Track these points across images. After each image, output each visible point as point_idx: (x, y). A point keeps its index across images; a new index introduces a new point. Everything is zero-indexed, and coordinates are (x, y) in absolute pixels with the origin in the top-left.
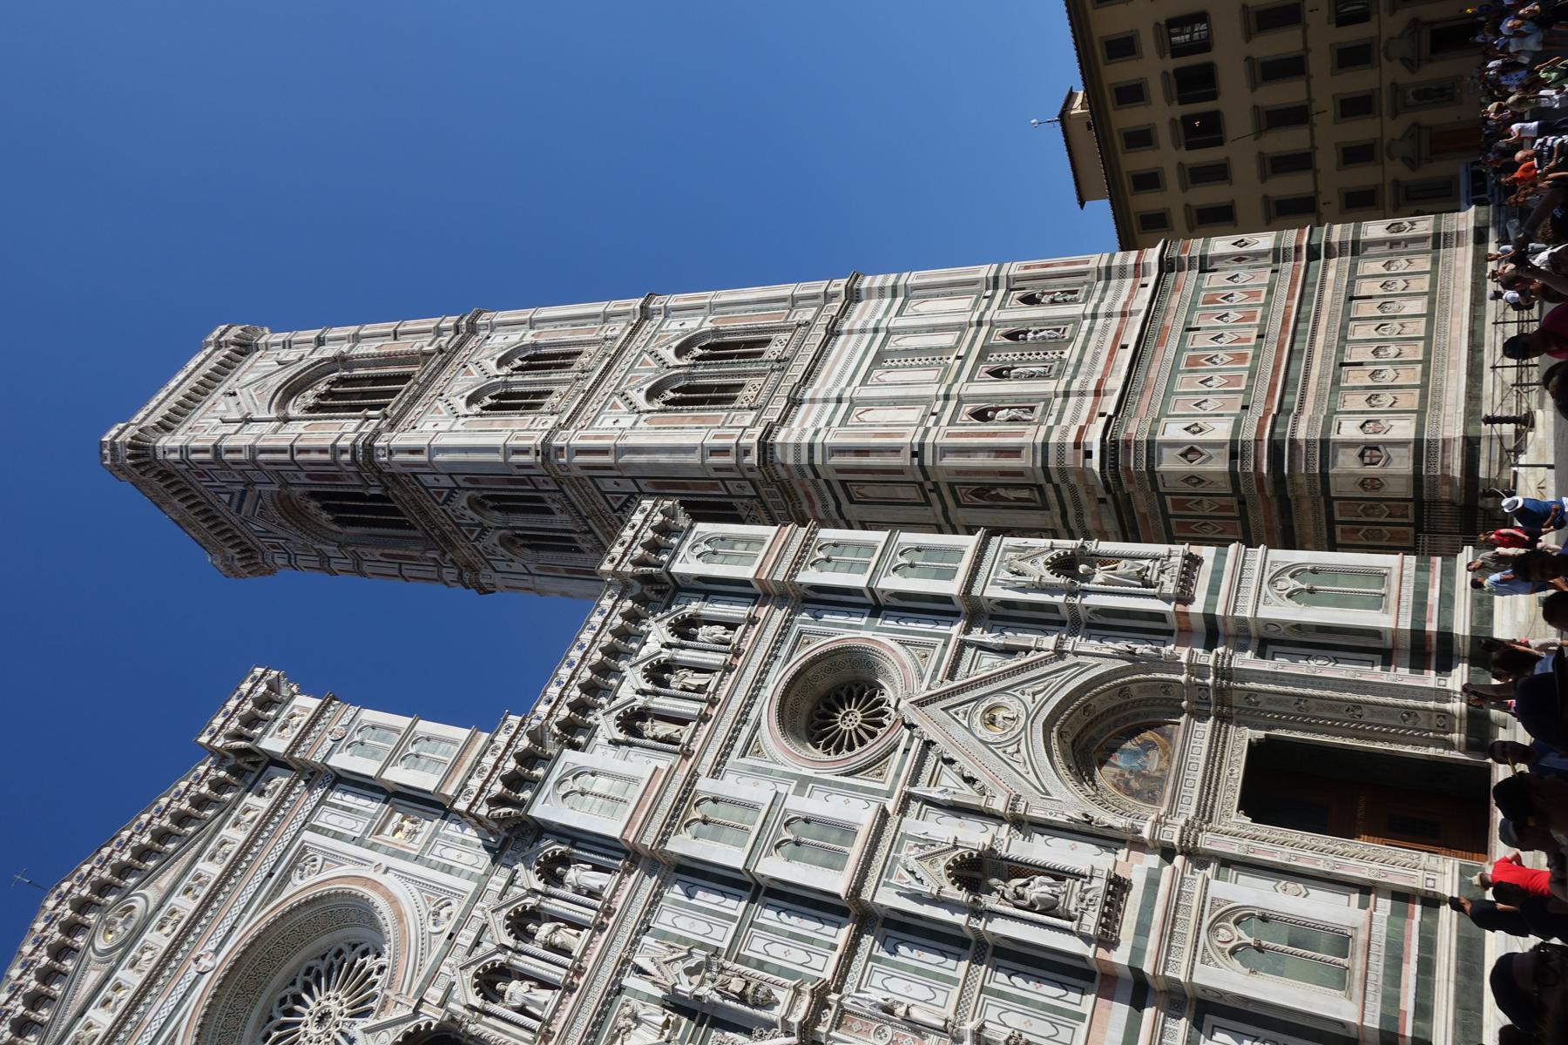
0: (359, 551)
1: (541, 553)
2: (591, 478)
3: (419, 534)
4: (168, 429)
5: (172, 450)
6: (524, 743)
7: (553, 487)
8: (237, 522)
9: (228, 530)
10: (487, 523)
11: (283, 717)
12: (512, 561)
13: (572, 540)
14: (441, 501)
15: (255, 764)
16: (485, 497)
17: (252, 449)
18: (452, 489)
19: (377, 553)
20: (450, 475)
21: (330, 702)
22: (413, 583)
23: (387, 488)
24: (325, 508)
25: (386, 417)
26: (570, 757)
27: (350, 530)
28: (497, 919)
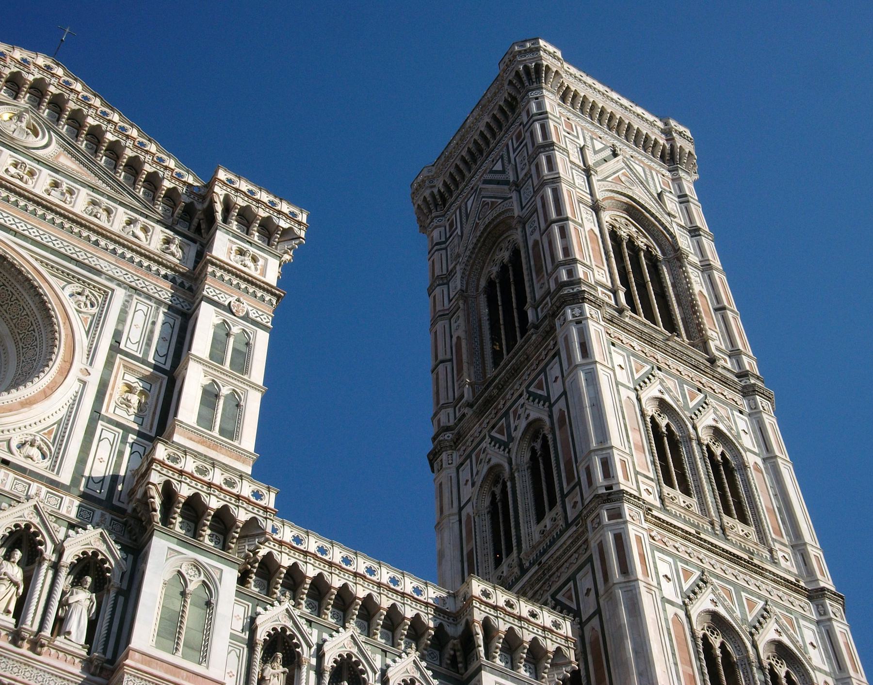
0: (460, 313)
1: (487, 518)
2: (590, 559)
3: (490, 373)
4: (563, 98)
5: (540, 105)
6: (242, 516)
7: (571, 516)
8: (473, 183)
9: (463, 177)
10: (514, 446)
11: (253, 250)
12: (473, 485)
13: (509, 551)
14: (531, 389)
15: (198, 230)
16: (545, 438)
17: (557, 179)
19: (461, 333)
20: (564, 393)
21: (273, 294)
22: (430, 377)
23: (536, 327)
24: (504, 268)
25: (620, 311)
26: (231, 575)
27: (483, 300)
28: (26, 513)
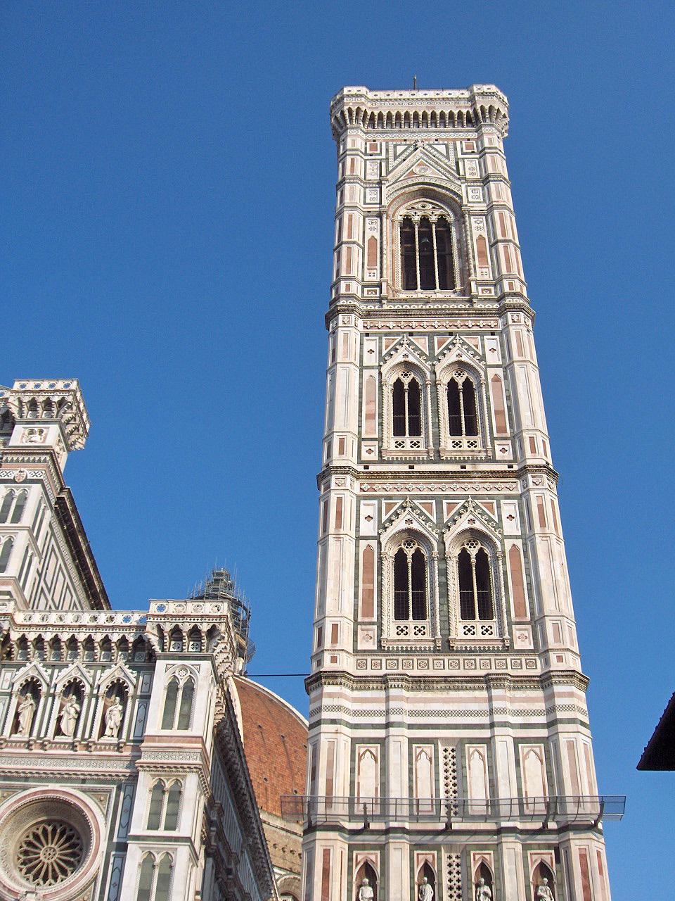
18: (483, 358)
